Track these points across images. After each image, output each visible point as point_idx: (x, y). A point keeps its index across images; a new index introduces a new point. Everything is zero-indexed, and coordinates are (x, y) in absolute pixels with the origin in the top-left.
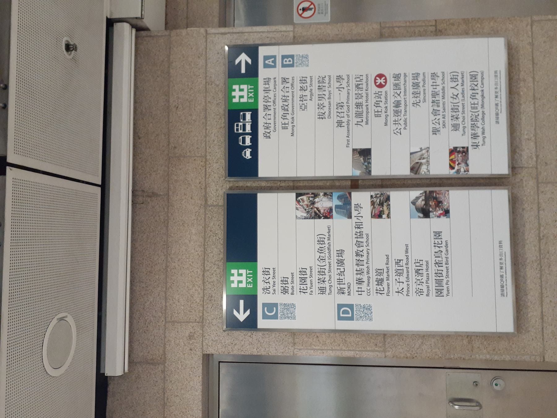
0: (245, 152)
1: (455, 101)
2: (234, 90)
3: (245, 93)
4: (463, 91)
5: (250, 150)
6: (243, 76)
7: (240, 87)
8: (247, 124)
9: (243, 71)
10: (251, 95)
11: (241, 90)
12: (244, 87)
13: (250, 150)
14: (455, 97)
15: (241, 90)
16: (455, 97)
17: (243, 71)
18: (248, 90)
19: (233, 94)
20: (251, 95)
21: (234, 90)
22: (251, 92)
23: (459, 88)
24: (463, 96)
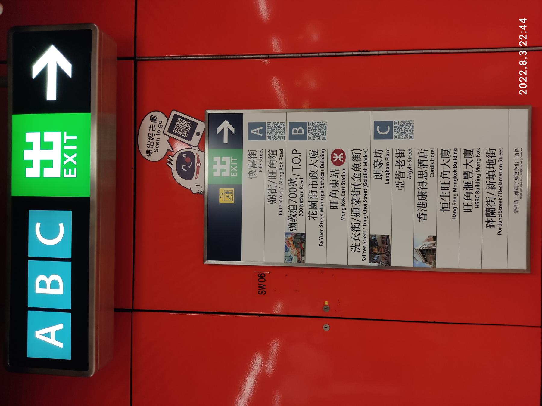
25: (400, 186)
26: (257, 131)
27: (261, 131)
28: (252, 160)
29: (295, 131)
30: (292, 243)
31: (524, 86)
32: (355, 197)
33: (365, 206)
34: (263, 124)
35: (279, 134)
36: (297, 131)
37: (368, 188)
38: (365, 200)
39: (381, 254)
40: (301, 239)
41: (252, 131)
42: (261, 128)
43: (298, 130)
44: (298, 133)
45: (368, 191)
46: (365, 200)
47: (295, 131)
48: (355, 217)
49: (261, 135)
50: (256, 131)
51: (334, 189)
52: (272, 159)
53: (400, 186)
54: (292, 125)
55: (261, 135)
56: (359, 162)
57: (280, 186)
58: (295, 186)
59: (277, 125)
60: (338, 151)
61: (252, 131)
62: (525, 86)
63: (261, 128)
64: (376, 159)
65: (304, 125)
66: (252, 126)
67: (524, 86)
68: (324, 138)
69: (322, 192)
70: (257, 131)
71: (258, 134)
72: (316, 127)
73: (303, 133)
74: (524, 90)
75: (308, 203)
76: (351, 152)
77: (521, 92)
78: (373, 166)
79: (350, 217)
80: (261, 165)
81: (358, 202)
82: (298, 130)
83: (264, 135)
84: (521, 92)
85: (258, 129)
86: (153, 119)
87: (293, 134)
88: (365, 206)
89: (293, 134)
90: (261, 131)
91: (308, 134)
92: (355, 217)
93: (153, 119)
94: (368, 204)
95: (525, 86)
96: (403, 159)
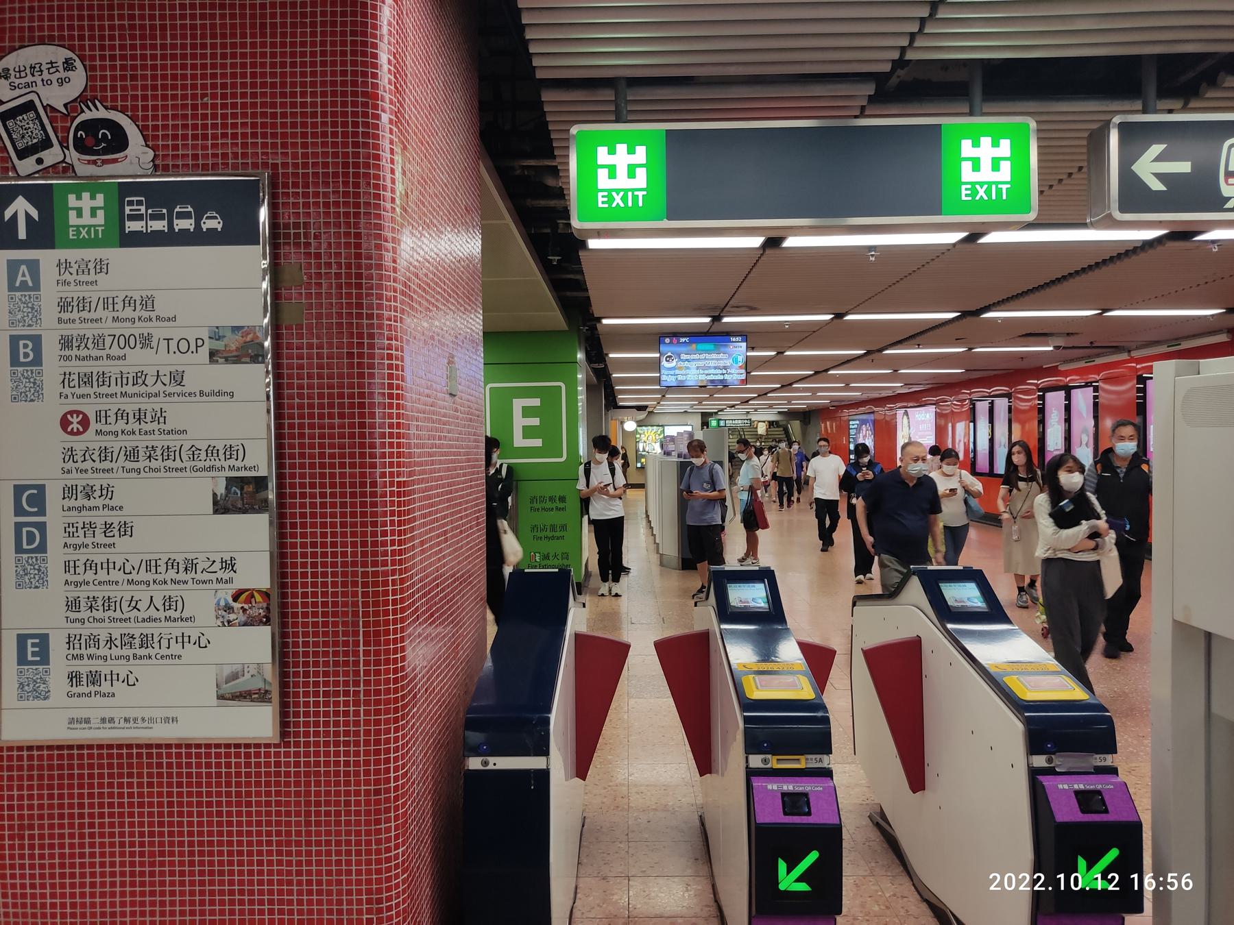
3: (87, 220)
4: (155, 620)
7: (100, 208)
10: (84, 233)
11: (93, 212)
12: (100, 218)
14: (133, 604)
15: (93, 212)
16: (133, 604)
20: (84, 233)
22: (88, 233)
23: (152, 611)
24: (144, 620)
25: (71, 530)
26: (24, 275)
27: (24, 283)
28: (91, 266)
29: (26, 346)
30: (249, 339)
31: (1010, 885)
32: (159, 452)
33: (158, 470)
34: (37, 287)
35: (19, 317)
36: (26, 349)
37: (188, 474)
38: (170, 469)
39: (242, 499)
40: (257, 356)
41: (23, 268)
42: (30, 284)
43: (28, 350)
44: (22, 350)
45: (184, 474)
46: (170, 469)
47: (26, 346)
48: (123, 453)
49: (18, 284)
50: (24, 275)
51: (131, 416)
52: (138, 303)
53: (71, 530)
54: (37, 340)
55: (18, 284)
56: (222, 456)
57: (110, 319)
58: (139, 346)
59: (36, 313)
60: (65, 423)
61: (23, 268)
62: (1010, 885)
63: (30, 284)
64: (97, 488)
65: (38, 361)
66: (34, 266)
67: (1010, 885)
68: (14, 399)
69: (156, 395)
70: (24, 275)
71: (20, 278)
72: (34, 383)
73: (22, 359)
74: (1001, 884)
75: (88, 370)
76: (239, 442)
78: (84, 483)
79: (123, 444)
80: (69, 284)
81: (150, 457)
82: (28, 350)
83: (18, 289)
85: (28, 278)
86: (68, 65)
87: (21, 343)
88: (158, 470)
89: (21, 343)
90: (24, 283)
91: (20, 369)
92: (123, 453)
93: (68, 65)
94: (162, 474)
95: (1010, 885)
96: (117, 534)
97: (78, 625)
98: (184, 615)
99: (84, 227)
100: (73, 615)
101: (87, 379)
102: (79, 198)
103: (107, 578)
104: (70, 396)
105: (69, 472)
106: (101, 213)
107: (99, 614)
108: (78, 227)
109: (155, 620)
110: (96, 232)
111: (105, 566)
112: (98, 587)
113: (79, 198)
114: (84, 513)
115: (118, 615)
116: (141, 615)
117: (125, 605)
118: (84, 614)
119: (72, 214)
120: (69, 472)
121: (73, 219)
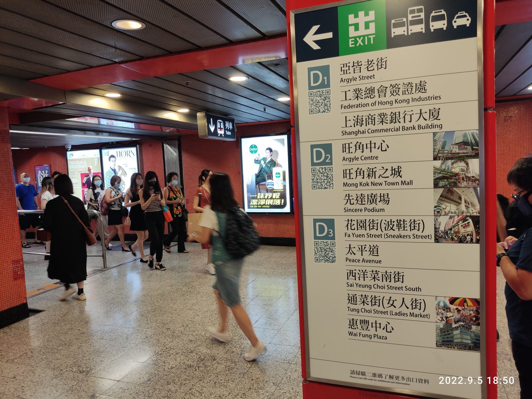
0: (465, 16)
1: (386, 302)
2: (367, 14)
3: (362, 31)
4: (404, 314)
5: (468, 23)
6: (336, 35)
8: (405, 28)
9: (329, 35)
10: (360, 41)
11: (367, 26)
13: (468, 23)
14: (391, 302)
15: (367, 26)
16: (391, 302)
17: (329, 35)
18: (368, 35)
19: (361, 14)
20: (360, 41)
21: (367, 14)
22: (363, 41)
24: (396, 314)
66: (325, 70)
77: (441, 379)
84: (441, 379)
97: (355, 313)
98: (423, 314)
99: (359, 37)
100: (353, 307)
101: (362, 225)
102: (356, 16)
103: (370, 155)
104: (351, 235)
105: (352, 285)
106: (372, 26)
107: (368, 307)
108: (355, 38)
109: (404, 314)
110: (369, 39)
111: (369, 146)
112: (364, 162)
113: (356, 16)
114: (359, 135)
115: (381, 309)
116: (395, 310)
117: (386, 302)
118: (359, 306)
119: (351, 29)
120: (352, 285)
121: (352, 33)
